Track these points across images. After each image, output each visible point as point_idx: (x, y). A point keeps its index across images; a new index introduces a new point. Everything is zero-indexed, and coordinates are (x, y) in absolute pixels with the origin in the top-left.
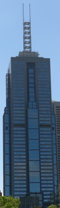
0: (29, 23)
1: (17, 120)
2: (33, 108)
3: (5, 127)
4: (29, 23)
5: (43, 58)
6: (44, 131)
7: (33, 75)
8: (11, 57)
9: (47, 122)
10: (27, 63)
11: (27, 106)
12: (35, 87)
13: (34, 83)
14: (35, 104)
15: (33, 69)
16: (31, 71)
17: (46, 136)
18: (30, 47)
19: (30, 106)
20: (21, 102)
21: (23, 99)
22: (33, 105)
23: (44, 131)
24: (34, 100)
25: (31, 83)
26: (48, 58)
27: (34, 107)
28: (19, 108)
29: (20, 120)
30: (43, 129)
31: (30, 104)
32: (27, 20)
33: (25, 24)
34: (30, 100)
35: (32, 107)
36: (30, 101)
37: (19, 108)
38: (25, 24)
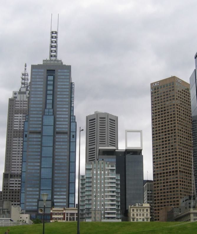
0: (56, 33)
1: (33, 128)
2: (49, 115)
3: (75, 137)
4: (56, 33)
5: (65, 65)
6: (33, 138)
7: (52, 82)
8: (32, 65)
9: (64, 129)
10: (47, 70)
11: (44, 114)
12: (47, 90)
13: (53, 90)
14: (52, 110)
15: (53, 76)
16: (50, 78)
17: (62, 143)
18: (55, 56)
19: (46, 113)
20: (38, 109)
21: (41, 106)
22: (49, 112)
23: (60, 138)
24: (51, 107)
25: (50, 90)
26: (69, 65)
27: (49, 114)
28: (36, 116)
29: (36, 128)
30: (60, 136)
31: (46, 110)
32: (54, 30)
33: (52, 33)
34: (47, 107)
35: (74, 120)
36: (47, 108)
37: (36, 116)
38: (52, 33)
